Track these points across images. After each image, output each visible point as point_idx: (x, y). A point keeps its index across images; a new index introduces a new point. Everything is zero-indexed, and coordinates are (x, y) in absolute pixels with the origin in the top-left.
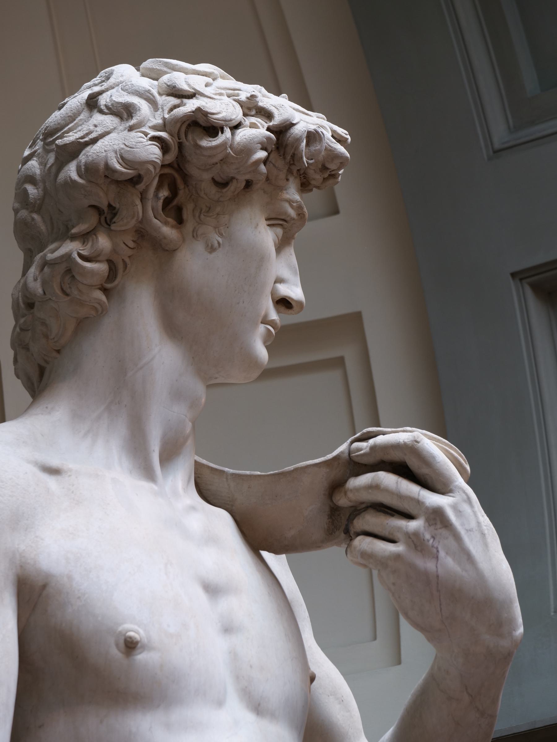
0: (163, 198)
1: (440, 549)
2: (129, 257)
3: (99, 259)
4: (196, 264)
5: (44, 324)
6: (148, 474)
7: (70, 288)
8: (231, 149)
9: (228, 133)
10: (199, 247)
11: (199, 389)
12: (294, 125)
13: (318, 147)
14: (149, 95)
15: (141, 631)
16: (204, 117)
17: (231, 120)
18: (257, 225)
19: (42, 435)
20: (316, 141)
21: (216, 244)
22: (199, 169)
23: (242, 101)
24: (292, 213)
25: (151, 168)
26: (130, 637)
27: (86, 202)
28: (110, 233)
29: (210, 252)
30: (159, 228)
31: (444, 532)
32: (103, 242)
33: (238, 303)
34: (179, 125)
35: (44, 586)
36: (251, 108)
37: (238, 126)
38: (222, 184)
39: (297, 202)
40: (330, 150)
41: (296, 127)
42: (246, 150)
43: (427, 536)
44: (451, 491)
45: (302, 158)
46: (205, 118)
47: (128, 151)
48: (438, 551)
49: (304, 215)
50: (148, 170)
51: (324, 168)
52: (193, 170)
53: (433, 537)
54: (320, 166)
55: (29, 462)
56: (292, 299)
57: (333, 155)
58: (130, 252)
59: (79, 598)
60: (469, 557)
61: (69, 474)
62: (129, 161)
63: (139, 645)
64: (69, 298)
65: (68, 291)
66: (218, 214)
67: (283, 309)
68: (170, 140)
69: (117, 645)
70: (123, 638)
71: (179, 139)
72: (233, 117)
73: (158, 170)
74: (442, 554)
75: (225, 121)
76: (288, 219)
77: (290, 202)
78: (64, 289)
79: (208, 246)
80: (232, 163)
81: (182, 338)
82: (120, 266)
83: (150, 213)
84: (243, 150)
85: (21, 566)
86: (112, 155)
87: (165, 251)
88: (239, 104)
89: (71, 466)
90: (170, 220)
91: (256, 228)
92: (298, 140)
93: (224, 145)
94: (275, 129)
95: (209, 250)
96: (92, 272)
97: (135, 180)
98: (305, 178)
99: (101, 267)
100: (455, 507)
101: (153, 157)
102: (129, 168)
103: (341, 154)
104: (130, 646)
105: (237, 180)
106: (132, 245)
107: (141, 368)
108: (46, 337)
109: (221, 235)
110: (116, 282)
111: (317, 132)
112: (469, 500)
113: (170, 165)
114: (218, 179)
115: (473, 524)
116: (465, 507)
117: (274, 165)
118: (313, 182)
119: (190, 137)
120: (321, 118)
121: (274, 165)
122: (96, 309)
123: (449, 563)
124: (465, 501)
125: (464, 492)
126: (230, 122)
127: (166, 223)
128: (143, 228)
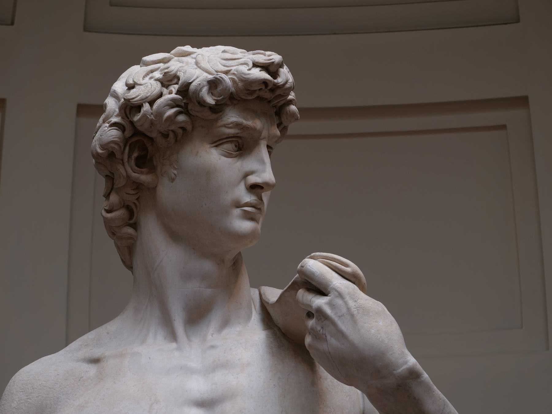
1: (327, 335)
4: (171, 192)
6: (173, 336)
9: (146, 107)
11: (208, 266)
17: (147, 98)
18: (198, 152)
19: (108, 333)
21: (173, 176)
24: (232, 131)
25: (113, 145)
29: (172, 182)
32: (114, 198)
34: (123, 111)
36: (168, 80)
37: (161, 95)
38: (165, 136)
39: (232, 123)
40: (245, 81)
41: (194, 84)
42: (159, 114)
43: (319, 328)
44: (329, 293)
51: (252, 92)
53: (322, 328)
55: (79, 361)
60: (341, 335)
67: (259, 190)
73: (121, 144)
74: (328, 337)
75: (143, 99)
76: (230, 136)
77: (225, 126)
82: (133, 207)
86: (97, 143)
89: (107, 354)
90: (143, 170)
91: (197, 155)
93: (145, 116)
94: (182, 90)
97: (111, 155)
100: (331, 304)
101: (111, 139)
105: (172, 131)
106: (132, 192)
109: (175, 169)
110: (135, 218)
111: (217, 78)
112: (340, 295)
115: (344, 310)
116: (339, 301)
117: (195, 111)
120: (256, 54)
121: (195, 111)
123: (333, 341)
124: (337, 297)
125: (336, 290)
127: (142, 173)
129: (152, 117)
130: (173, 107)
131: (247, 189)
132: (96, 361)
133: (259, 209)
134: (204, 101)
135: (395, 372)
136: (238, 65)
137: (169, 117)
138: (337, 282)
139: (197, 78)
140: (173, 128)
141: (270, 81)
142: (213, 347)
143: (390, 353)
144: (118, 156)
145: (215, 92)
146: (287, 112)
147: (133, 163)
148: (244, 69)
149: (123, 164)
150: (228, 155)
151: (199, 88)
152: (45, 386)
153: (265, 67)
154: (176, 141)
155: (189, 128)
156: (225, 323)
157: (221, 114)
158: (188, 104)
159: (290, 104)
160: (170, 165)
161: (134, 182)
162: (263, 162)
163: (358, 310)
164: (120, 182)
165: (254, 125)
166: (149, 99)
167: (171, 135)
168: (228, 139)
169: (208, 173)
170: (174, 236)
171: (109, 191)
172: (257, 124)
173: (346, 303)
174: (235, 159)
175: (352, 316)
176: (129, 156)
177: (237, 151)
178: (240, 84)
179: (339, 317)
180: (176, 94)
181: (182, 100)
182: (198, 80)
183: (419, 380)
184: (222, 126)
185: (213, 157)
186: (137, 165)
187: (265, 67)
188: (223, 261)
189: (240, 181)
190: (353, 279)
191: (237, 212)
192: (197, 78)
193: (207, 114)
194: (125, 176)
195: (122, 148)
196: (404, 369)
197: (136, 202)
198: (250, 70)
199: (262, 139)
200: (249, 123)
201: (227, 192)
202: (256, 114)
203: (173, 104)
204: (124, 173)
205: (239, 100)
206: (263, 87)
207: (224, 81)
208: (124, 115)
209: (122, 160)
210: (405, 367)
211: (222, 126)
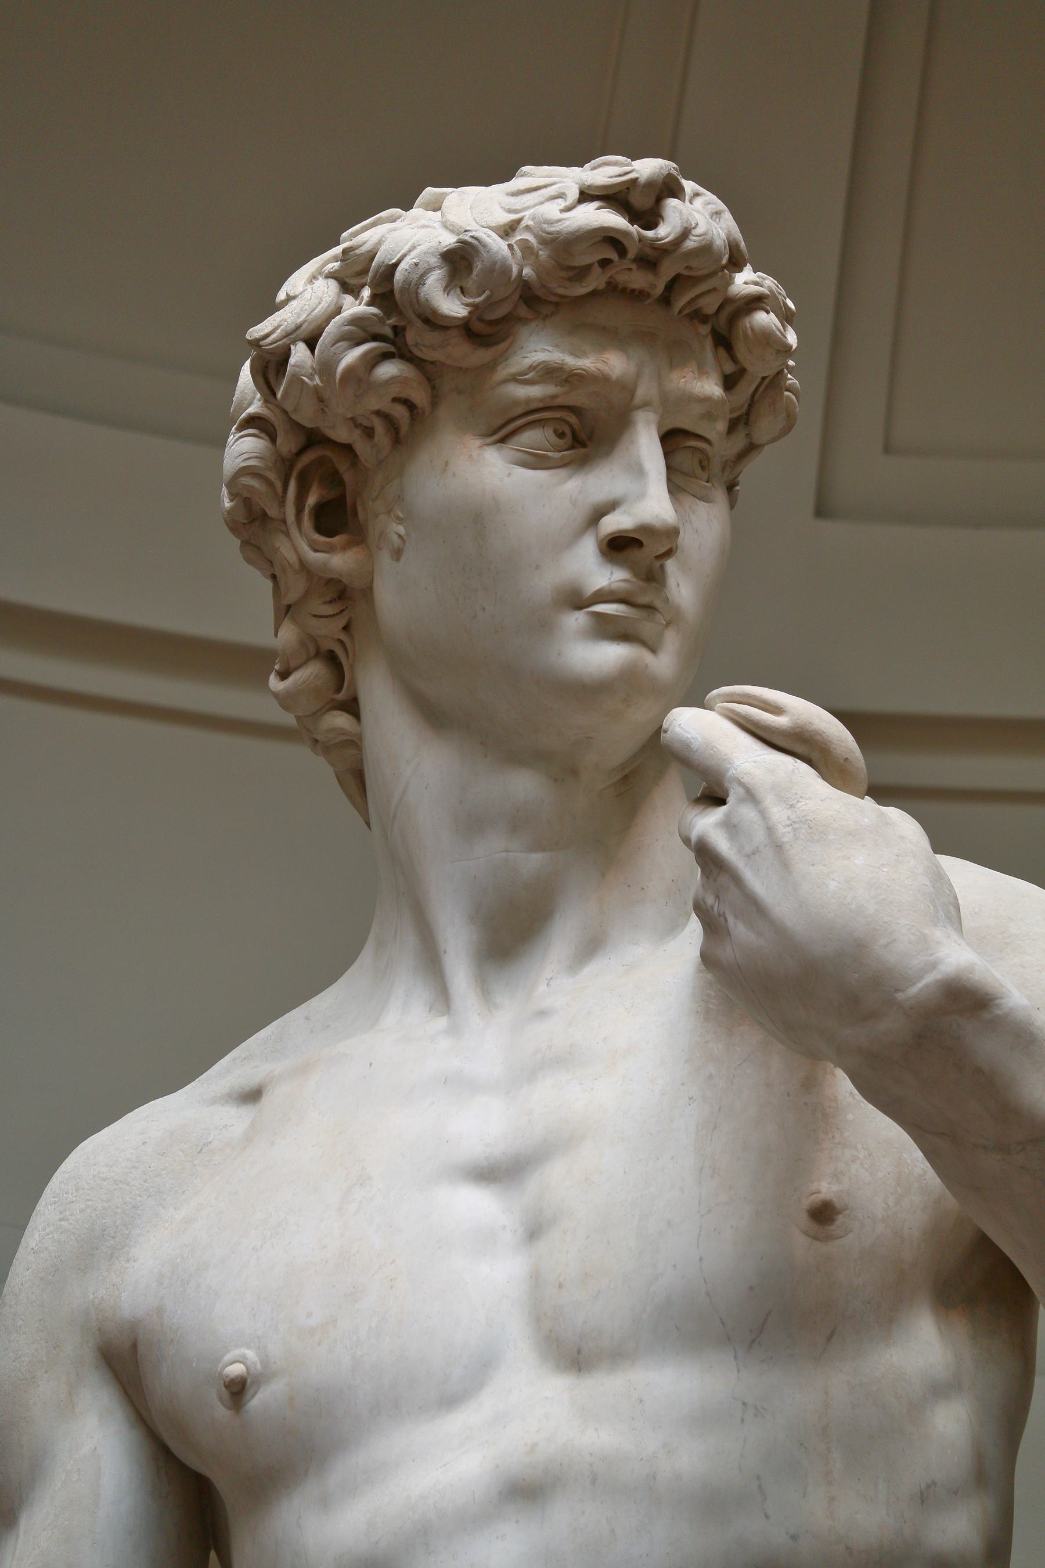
2: (346, 628)
3: (293, 664)
9: (299, 353)
10: (384, 559)
11: (524, 786)
12: (396, 265)
15: (251, 1354)
17: (298, 327)
18: (447, 464)
23: (336, 271)
24: (535, 391)
29: (398, 559)
31: (724, 879)
33: (475, 617)
34: (261, 381)
35: (134, 1346)
39: (532, 368)
40: (553, 240)
48: (726, 920)
51: (581, 273)
53: (717, 897)
54: (563, 274)
55: (215, 1101)
56: (626, 531)
57: (563, 246)
58: (342, 622)
63: (249, 1381)
66: (383, 487)
67: (634, 554)
73: (272, 476)
74: (731, 920)
75: (287, 335)
76: (534, 406)
77: (515, 379)
90: (337, 540)
91: (444, 471)
99: (310, 673)
104: (237, 1390)
105: (378, 413)
106: (328, 610)
109: (400, 521)
112: (751, 796)
115: (760, 835)
120: (599, 166)
124: (741, 801)
125: (741, 783)
126: (298, 332)
127: (330, 549)
129: (317, 380)
130: (359, 344)
132: (252, 1096)
133: (649, 608)
134: (435, 312)
135: (900, 996)
136: (542, 203)
137: (350, 370)
138: (747, 759)
139: (413, 248)
141: (626, 234)
142: (542, 1014)
143: (882, 942)
144: (272, 512)
145: (470, 284)
146: (746, 335)
148: (552, 210)
150: (536, 462)
151: (415, 277)
152: (105, 1180)
153: (612, 197)
154: (397, 439)
155: (420, 396)
156: (591, 946)
157: (503, 346)
158: (404, 329)
159: (756, 309)
160: (389, 512)
161: (330, 581)
162: (639, 471)
163: (795, 830)
165: (600, 365)
166: (304, 331)
168: (533, 415)
169: (478, 519)
170: (434, 716)
172: (614, 363)
173: (763, 814)
174: (562, 473)
175: (778, 847)
177: (572, 448)
179: (748, 856)
180: (369, 304)
181: (381, 320)
182: (413, 254)
183: (986, 1015)
184: (506, 381)
185: (487, 472)
186: (319, 529)
187: (612, 197)
188: (574, 772)
189: (579, 534)
190: (799, 748)
191: (576, 620)
192: (413, 248)
193: (461, 352)
194: (297, 565)
196: (927, 986)
197: (343, 637)
198: (568, 209)
199: (638, 408)
200: (587, 363)
201: (538, 567)
202: (610, 337)
203: (360, 331)
204: (292, 557)
205: (557, 304)
207: (485, 246)
209: (284, 521)
210: (929, 978)
211: (506, 381)
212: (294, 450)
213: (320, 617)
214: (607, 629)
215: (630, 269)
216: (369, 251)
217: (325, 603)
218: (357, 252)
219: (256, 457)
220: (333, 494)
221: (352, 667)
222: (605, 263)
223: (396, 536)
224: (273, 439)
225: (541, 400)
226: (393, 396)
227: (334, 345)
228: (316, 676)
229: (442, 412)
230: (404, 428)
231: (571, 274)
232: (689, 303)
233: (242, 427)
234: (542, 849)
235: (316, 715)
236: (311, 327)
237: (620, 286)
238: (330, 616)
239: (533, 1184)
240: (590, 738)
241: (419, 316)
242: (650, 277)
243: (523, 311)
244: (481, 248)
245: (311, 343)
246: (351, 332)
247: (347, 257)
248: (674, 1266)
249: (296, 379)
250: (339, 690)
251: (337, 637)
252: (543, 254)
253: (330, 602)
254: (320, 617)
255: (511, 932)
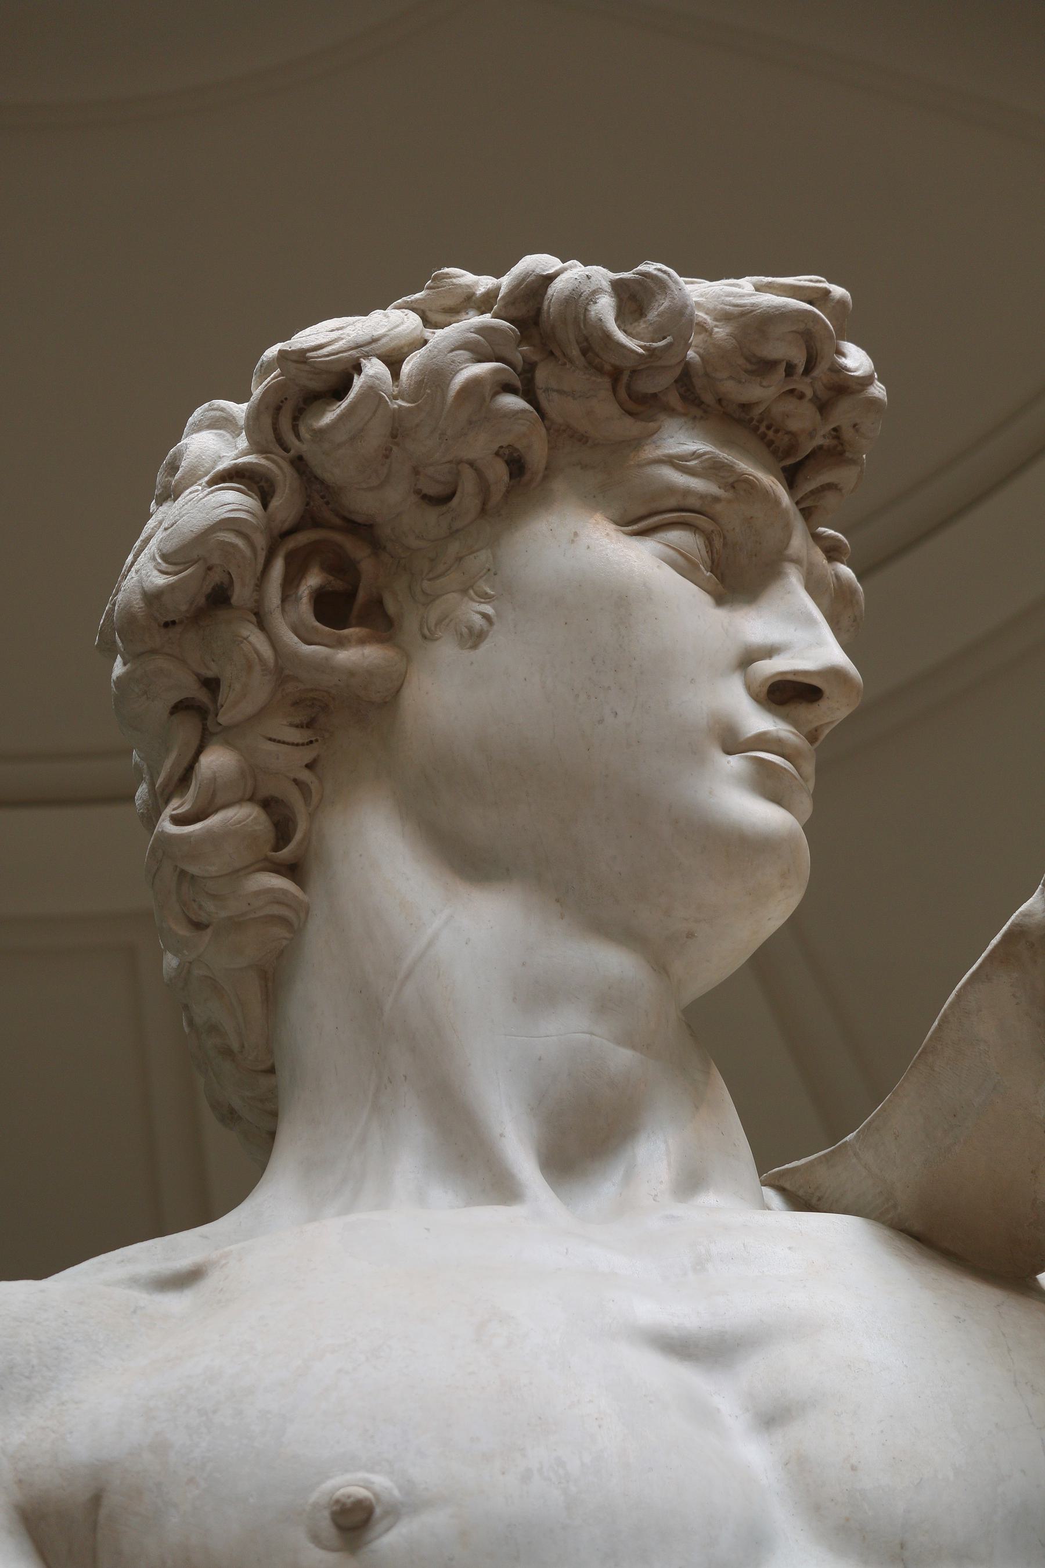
0: (307, 592)
2: (309, 766)
5: (213, 1029)
6: (502, 1188)
7: (200, 907)
8: (403, 400)
9: (375, 368)
10: (446, 650)
12: (551, 278)
13: (666, 303)
14: (212, 413)
16: (302, 366)
17: (374, 340)
20: (653, 295)
21: (478, 621)
22: (370, 489)
26: (337, 1501)
27: (161, 706)
28: (228, 735)
29: (475, 646)
30: (327, 659)
32: (216, 761)
33: (601, 721)
34: (267, 421)
35: (96, 1500)
39: (695, 455)
40: (743, 314)
42: (434, 378)
45: (608, 336)
46: (307, 368)
47: (168, 535)
49: (747, 481)
50: (223, 544)
51: (764, 367)
52: (364, 503)
54: (741, 361)
57: (753, 324)
58: (307, 755)
59: (191, 1481)
61: (224, 1262)
62: (176, 552)
63: (378, 1511)
64: (209, 931)
65: (203, 918)
66: (459, 559)
68: (263, 462)
69: (316, 1539)
70: (326, 1513)
71: (287, 450)
72: (381, 331)
73: (261, 541)
75: (358, 346)
76: (692, 502)
77: (672, 461)
78: (194, 918)
79: (461, 634)
80: (417, 425)
81: (508, 870)
82: (295, 797)
83: (291, 639)
84: (422, 381)
85: (20, 1481)
87: (372, 708)
88: (413, 310)
92: (577, 302)
95: (469, 644)
96: (211, 838)
98: (777, 431)
101: (223, 513)
102: (181, 567)
103: (777, 308)
105: (471, 464)
107: (407, 977)
108: (227, 1052)
109: (486, 598)
110: (298, 836)
113: (308, 520)
114: (433, 490)
117: (560, 392)
118: (794, 425)
119: (302, 430)
122: (284, 921)
126: (374, 345)
127: (341, 643)
128: (312, 690)
131: (756, 698)
140: (480, 446)
144: (241, 594)
145: (641, 326)
147: (305, 608)
149: (262, 624)
150: (686, 567)
151: (587, 290)
155: (537, 454)
164: (245, 696)
166: (383, 345)
167: (468, 484)
169: (622, 602)
171: (185, 764)
176: (286, 596)
178: (721, 332)
186: (320, 616)
193: (603, 412)
195: (261, 560)
197: (305, 776)
201: (692, 681)
206: (799, 359)
208: (271, 437)
212: (286, 526)
213: (279, 742)
214: (768, 784)
215: (801, 396)
216: (468, 286)
217: (291, 725)
218: (454, 280)
219: (248, 511)
220: (338, 585)
221: (312, 816)
222: (790, 369)
223: (479, 616)
224: (265, 505)
225: (703, 497)
226: (505, 440)
227: (452, 351)
228: (255, 818)
229: (558, 485)
230: (496, 497)
231: (749, 367)
232: (812, 492)
233: (212, 483)
234: (633, 1047)
235: (238, 873)
236: (393, 344)
237: (763, 429)
238: (293, 744)
239: (754, 1372)
240: (690, 935)
241: (578, 343)
242: (818, 417)
243: (673, 399)
244: (670, 283)
245: (394, 362)
246: (477, 343)
247: (439, 284)
248: (1023, 1471)
249: (371, 392)
250: (277, 848)
251: (292, 775)
252: (721, 332)
253: (297, 726)
254: (279, 742)
255: (583, 1139)
